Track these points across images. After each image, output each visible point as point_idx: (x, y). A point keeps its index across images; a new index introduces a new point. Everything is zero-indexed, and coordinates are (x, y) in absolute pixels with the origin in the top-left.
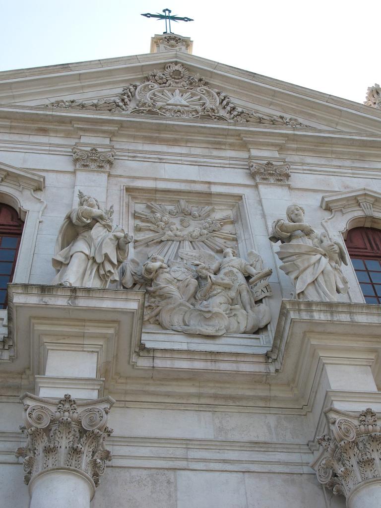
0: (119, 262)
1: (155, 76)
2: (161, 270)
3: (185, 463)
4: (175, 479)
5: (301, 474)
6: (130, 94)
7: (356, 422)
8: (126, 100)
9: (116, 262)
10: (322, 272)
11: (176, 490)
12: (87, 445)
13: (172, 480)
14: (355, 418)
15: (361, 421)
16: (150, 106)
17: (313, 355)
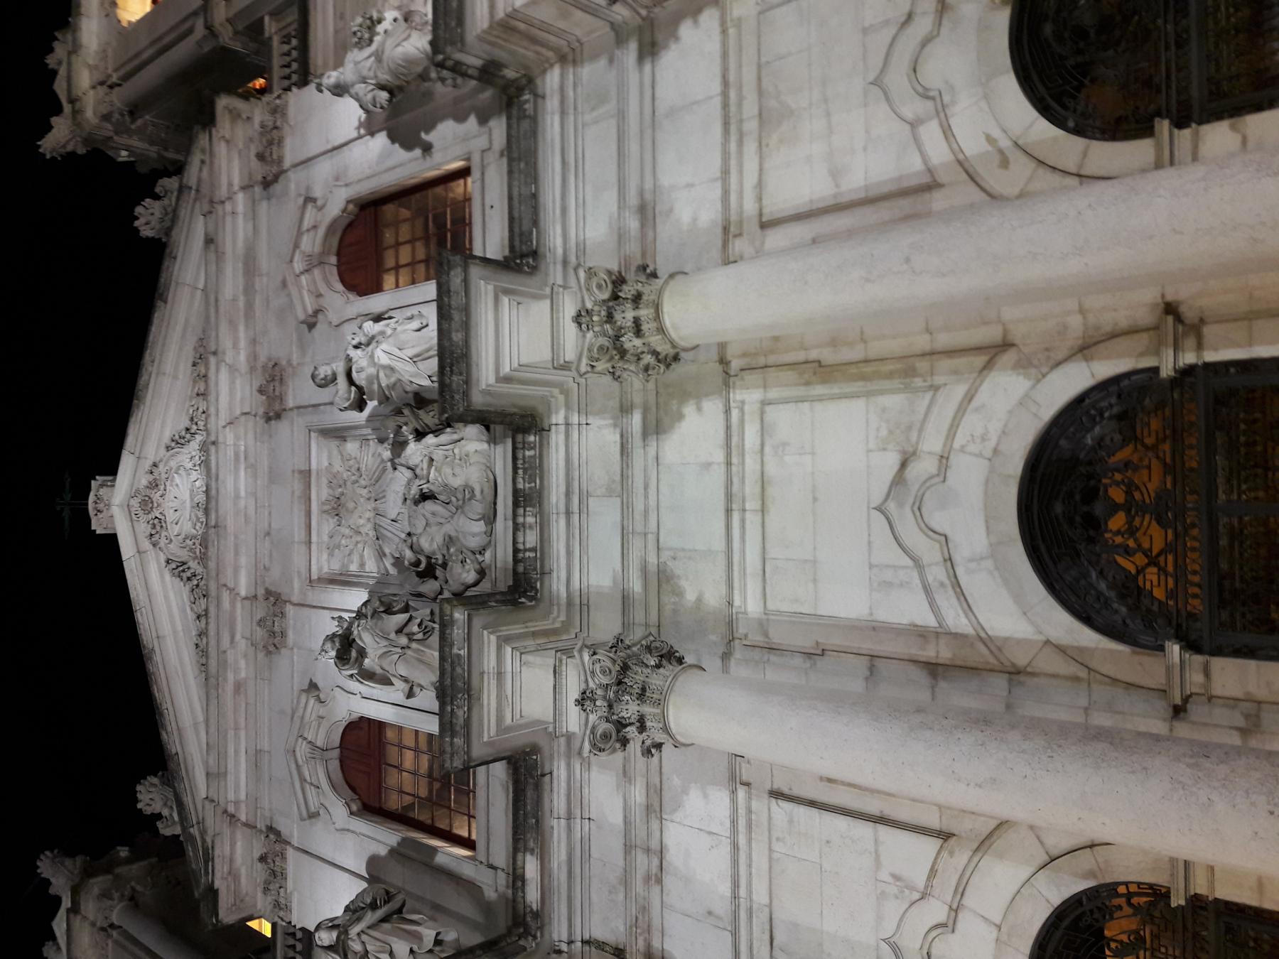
0: (406, 609)
1: (151, 535)
2: (414, 546)
3: (650, 536)
4: (671, 549)
5: (657, 392)
6: (181, 569)
7: (590, 335)
8: (188, 574)
9: (406, 616)
10: (400, 349)
11: (683, 550)
12: (633, 676)
13: (671, 553)
14: (584, 336)
15: (588, 329)
16: (194, 544)
17: (507, 379)
